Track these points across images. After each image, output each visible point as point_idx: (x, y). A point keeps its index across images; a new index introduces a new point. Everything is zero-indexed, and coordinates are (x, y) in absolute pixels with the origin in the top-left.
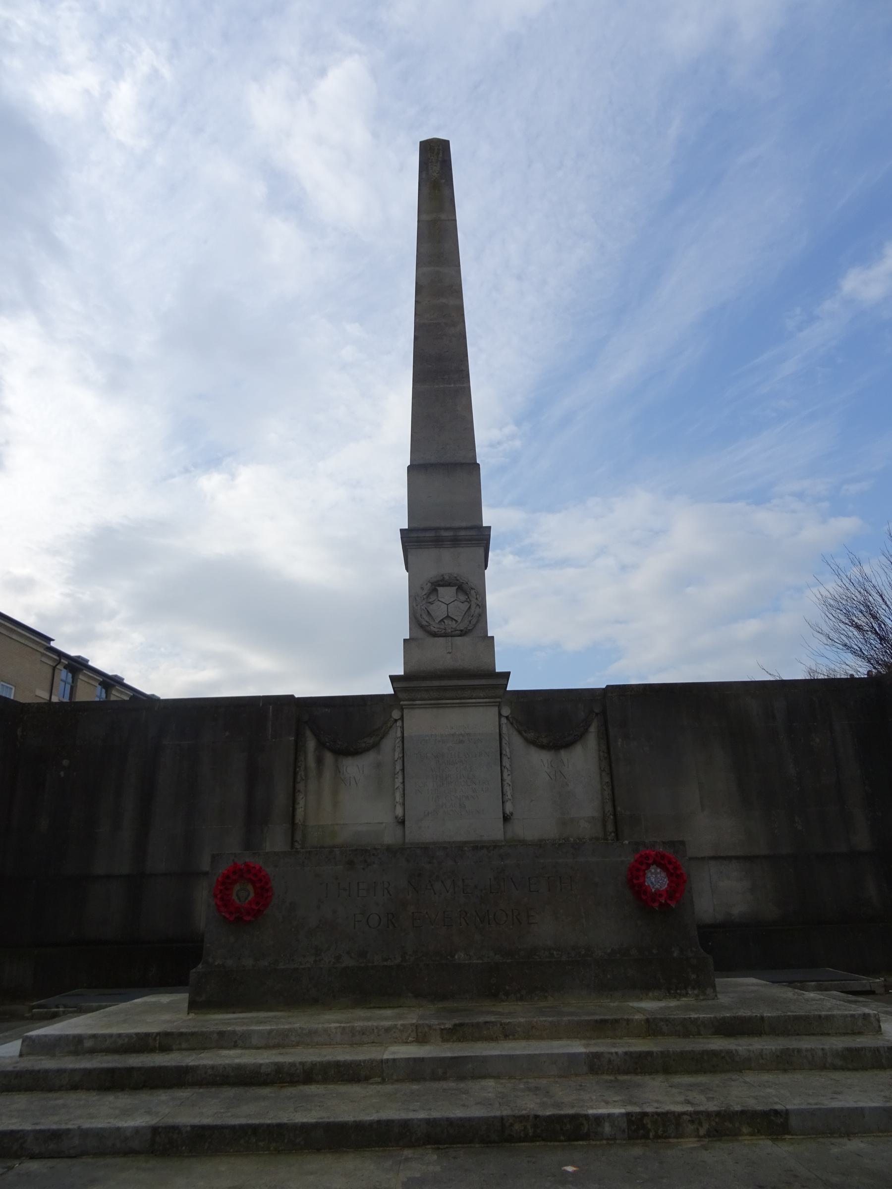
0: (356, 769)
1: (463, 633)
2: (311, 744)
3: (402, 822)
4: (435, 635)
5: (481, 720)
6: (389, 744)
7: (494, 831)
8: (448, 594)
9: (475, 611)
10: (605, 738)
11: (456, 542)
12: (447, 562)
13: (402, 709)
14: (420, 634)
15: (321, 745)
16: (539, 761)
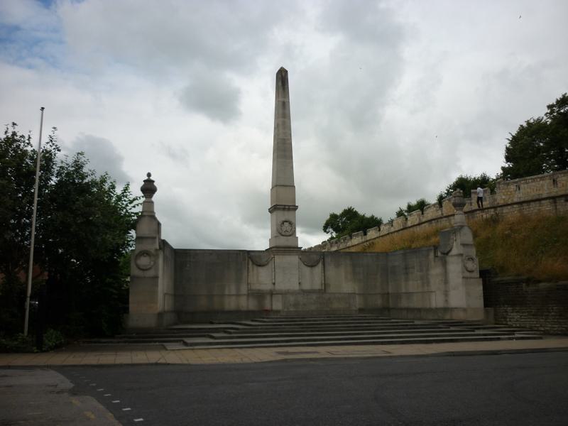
0: (261, 269)
1: (290, 236)
2: (250, 263)
3: (274, 284)
4: (283, 235)
5: (294, 259)
6: (270, 265)
7: (297, 287)
8: (286, 224)
9: (293, 230)
10: (324, 265)
11: (289, 209)
12: (286, 215)
13: (274, 255)
14: (279, 235)
15: (253, 263)
16: (307, 270)
